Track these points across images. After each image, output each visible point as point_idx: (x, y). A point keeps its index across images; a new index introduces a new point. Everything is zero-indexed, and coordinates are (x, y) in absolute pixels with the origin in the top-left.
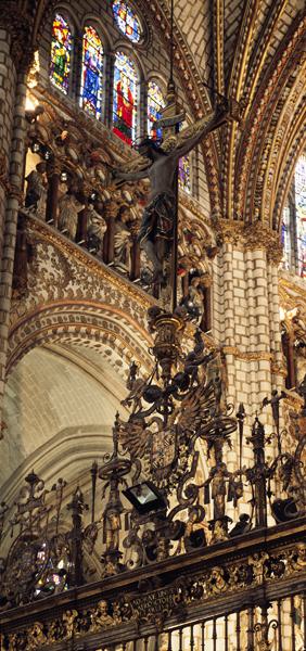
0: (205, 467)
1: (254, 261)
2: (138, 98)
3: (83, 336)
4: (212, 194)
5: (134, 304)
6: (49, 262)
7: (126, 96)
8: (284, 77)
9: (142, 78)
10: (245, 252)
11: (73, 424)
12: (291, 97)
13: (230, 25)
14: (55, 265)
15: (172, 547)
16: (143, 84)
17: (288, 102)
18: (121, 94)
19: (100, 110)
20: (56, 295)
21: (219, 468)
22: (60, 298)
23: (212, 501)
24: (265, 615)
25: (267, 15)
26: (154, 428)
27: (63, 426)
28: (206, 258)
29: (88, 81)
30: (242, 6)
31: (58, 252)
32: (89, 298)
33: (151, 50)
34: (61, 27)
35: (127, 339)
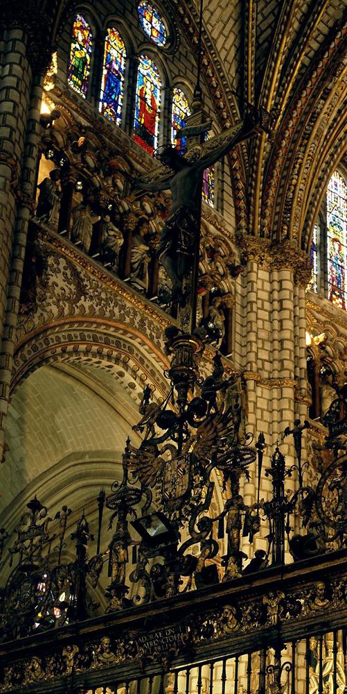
0: (220, 498)
1: (280, 282)
2: (162, 105)
3: (94, 356)
4: (237, 209)
5: (151, 323)
6: (60, 276)
7: (149, 102)
8: (319, 88)
11: (80, 448)
13: (262, 32)
14: (66, 279)
15: (182, 582)
17: (322, 115)
18: (144, 100)
19: (120, 116)
20: (66, 311)
21: (235, 501)
22: (71, 314)
23: (226, 535)
24: (278, 656)
26: (168, 456)
27: (70, 450)
28: (229, 277)
29: (108, 85)
30: (276, 12)
31: (70, 265)
32: (102, 315)
33: (177, 54)
34: (82, 28)
35: (142, 361)
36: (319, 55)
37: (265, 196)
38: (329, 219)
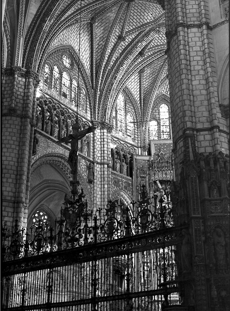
0: (83, 224)
1: (103, 133)
4: (91, 112)
8: (113, 76)
9: (71, 78)
10: (101, 130)
11: (48, 178)
12: (115, 82)
13: (97, 60)
16: (71, 81)
17: (114, 84)
21: (86, 226)
25: (108, 58)
26: (71, 212)
27: (45, 179)
33: (73, 69)
36: (113, 66)
37: (99, 107)
38: (118, 108)
